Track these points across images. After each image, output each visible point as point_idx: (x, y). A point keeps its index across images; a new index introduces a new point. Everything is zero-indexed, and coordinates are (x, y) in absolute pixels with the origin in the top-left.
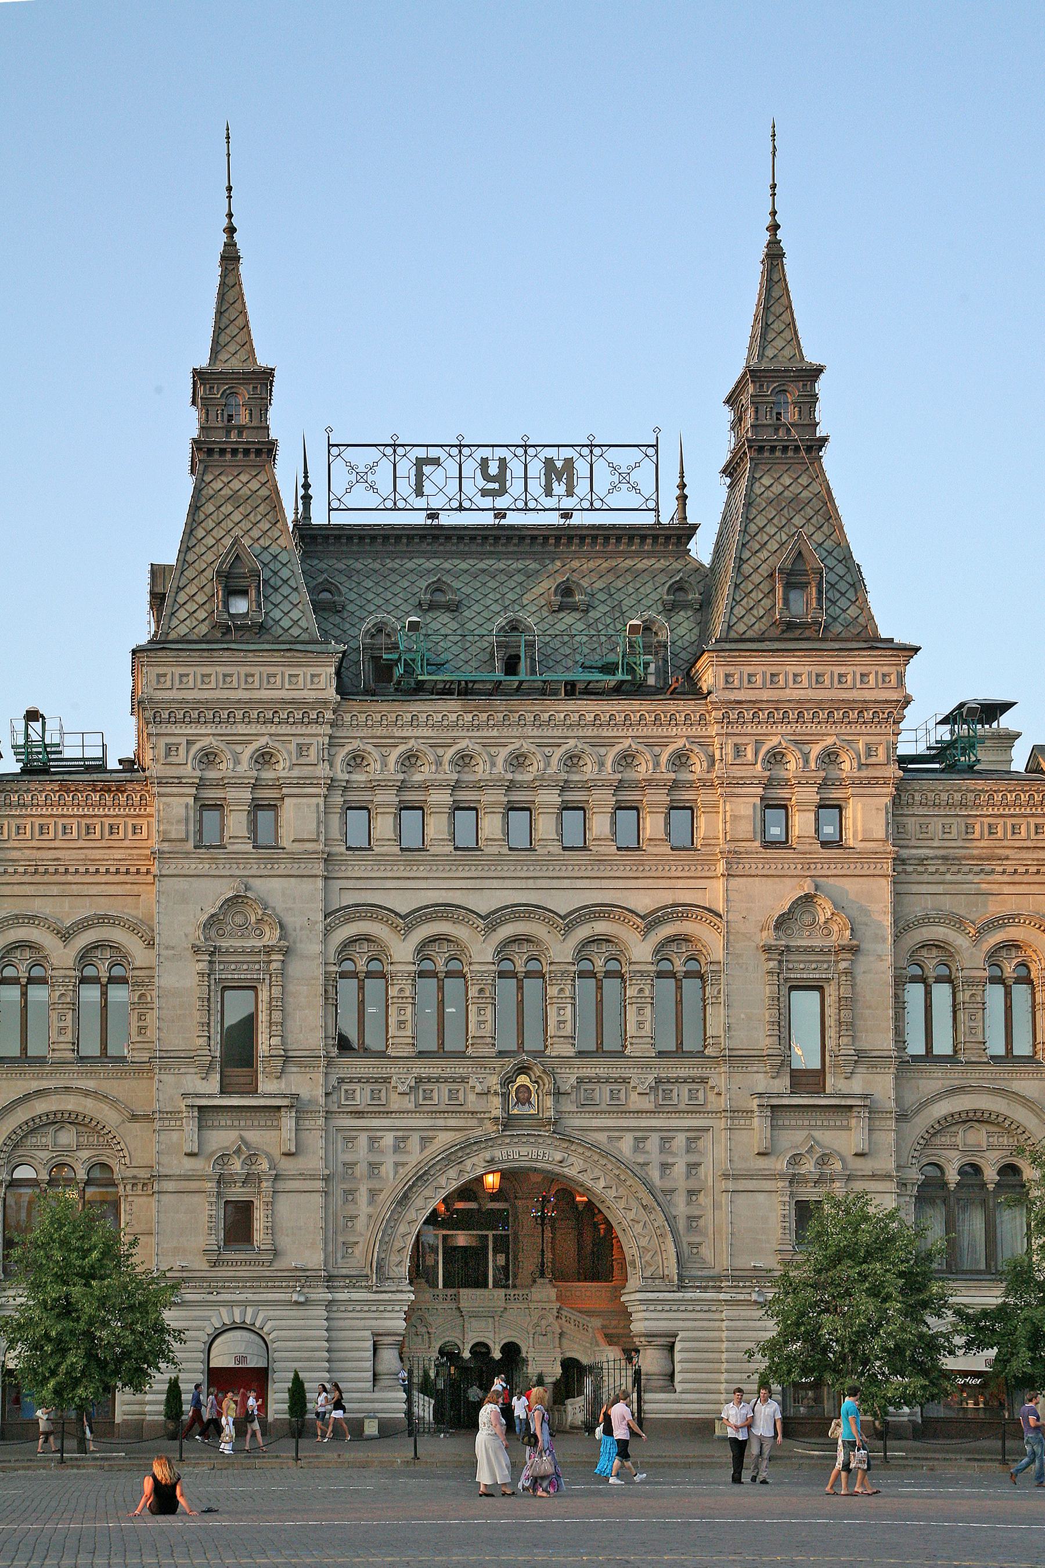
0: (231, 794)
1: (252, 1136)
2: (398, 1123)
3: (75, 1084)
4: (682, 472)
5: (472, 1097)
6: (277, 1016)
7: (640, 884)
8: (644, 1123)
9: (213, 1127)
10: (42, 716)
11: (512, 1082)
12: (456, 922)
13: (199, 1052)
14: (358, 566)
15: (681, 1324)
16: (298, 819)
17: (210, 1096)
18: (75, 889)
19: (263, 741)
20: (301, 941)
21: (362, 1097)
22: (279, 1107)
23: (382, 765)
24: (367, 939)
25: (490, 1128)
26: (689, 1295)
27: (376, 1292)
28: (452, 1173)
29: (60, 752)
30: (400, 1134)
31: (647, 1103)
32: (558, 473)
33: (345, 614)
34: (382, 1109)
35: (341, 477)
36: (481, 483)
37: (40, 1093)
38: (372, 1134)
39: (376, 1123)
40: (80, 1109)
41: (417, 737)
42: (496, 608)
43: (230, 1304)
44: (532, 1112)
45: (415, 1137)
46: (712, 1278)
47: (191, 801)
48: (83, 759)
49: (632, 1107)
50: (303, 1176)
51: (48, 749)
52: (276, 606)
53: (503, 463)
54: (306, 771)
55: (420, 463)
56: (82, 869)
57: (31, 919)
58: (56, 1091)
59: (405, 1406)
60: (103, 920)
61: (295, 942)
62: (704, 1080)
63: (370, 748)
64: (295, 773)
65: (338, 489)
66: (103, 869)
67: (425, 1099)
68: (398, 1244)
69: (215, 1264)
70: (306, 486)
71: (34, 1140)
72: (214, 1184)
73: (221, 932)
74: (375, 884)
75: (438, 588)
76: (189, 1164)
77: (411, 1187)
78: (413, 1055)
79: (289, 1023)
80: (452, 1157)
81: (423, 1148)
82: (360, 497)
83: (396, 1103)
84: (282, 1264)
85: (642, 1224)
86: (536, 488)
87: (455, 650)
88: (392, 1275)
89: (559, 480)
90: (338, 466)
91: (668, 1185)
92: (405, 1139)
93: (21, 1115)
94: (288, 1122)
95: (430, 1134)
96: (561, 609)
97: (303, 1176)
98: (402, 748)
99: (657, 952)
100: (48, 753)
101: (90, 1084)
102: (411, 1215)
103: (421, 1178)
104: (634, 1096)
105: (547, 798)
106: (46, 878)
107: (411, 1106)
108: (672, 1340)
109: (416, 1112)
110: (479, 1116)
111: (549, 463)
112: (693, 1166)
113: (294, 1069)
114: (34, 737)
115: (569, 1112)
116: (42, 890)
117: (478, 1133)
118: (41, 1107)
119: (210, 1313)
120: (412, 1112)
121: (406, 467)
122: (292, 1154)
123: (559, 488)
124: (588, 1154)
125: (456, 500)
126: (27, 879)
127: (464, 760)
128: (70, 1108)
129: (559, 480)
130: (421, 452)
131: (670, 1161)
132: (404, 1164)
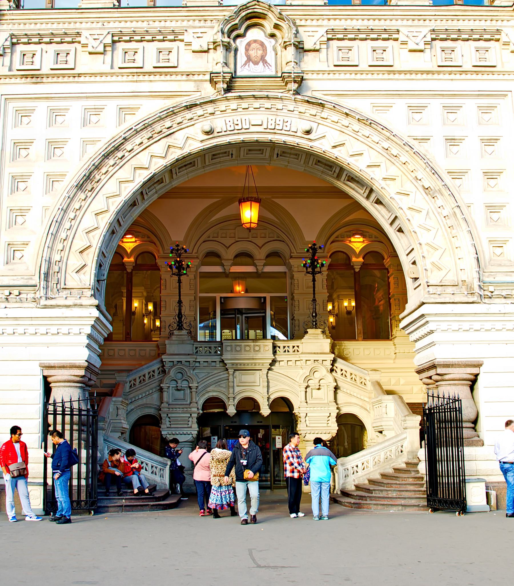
11: (238, 36)
25: (209, 91)
26: (494, 308)
27: (45, 307)
68: (79, 243)
77: (98, 167)
83: (86, 63)
85: (424, 212)
88: (69, 285)
92: (98, 111)
102: (99, 203)
107: (106, 68)
108: (475, 371)
110: (196, 77)
115: (318, 72)
120: (106, 74)
132: (93, 142)
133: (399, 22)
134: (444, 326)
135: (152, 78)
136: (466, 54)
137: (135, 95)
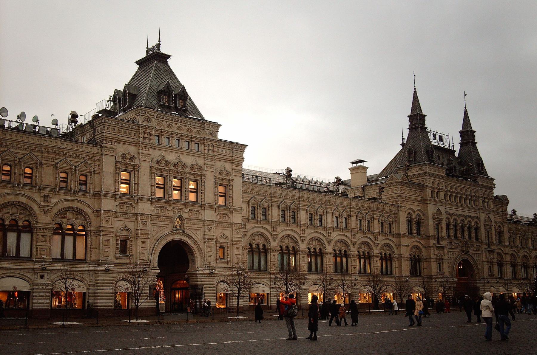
22: (443, 247)
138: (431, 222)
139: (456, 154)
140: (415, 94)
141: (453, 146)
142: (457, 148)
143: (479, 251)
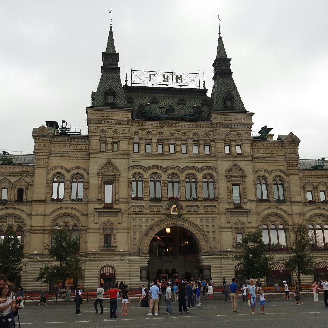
0: (108, 140)
1: (111, 219)
2: (145, 216)
3: (69, 206)
4: (204, 79)
5: (163, 210)
6: (117, 190)
7: (200, 161)
8: (202, 216)
9: (102, 217)
10: (66, 123)
12: (158, 169)
13: (99, 199)
14: (137, 94)
15: (212, 263)
16: (123, 145)
17: (100, 209)
18: (71, 161)
19: (115, 128)
20: (123, 173)
21: (137, 210)
22: (117, 212)
23: (143, 133)
24: (139, 173)
26: (214, 256)
27: (141, 257)
28: (158, 228)
29: (70, 131)
30: (146, 218)
31: (202, 211)
32: (179, 78)
33: (134, 104)
34: (142, 212)
35: (134, 77)
36: (163, 79)
37: (61, 208)
38: (140, 218)
39: (140, 216)
40: (71, 212)
41: (150, 128)
42: (166, 103)
43: (106, 260)
44: (176, 213)
45: (150, 219)
46: (218, 252)
47: (98, 141)
48: (76, 133)
49: (199, 212)
50: (123, 228)
51: (67, 130)
52: (119, 100)
53: (168, 76)
54: (124, 135)
55: (150, 75)
56: (73, 156)
57: (61, 167)
58: (66, 208)
59: (148, 285)
60: (78, 168)
61: (122, 173)
62: (215, 206)
63: (139, 131)
64: (122, 135)
65: (133, 79)
66: (78, 156)
67: (152, 210)
68: (145, 245)
69: (102, 250)
70: (126, 78)
71: (60, 220)
72: (102, 230)
73: (105, 171)
74: (140, 161)
75: (155, 99)
76: (96, 226)
78: (149, 200)
79: (120, 192)
80: (158, 224)
81: (152, 222)
82: (138, 81)
84: (117, 250)
86: (175, 81)
87: (158, 111)
89: (179, 79)
90: (133, 75)
91: (208, 230)
92: (147, 220)
93: (57, 213)
94: (120, 216)
95: (153, 218)
96: (181, 104)
97: (123, 228)
98: (146, 131)
99: (203, 177)
100: (67, 131)
101: (74, 206)
102: (148, 238)
103: (151, 228)
104: (199, 210)
105: (178, 142)
106: (65, 158)
109: (150, 213)
111: (177, 76)
112: (213, 226)
113: (121, 203)
114: (63, 126)
116: (64, 160)
117: (164, 218)
118: (62, 211)
119: (101, 262)
121: (148, 76)
122: (121, 223)
123: (179, 81)
124: (189, 223)
125: (157, 82)
126: (60, 158)
127: (160, 134)
128: (68, 212)
129: (179, 79)
130: (151, 73)
131: (208, 224)
132: (147, 226)
133: (199, 204)
134: (205, 260)
135: (157, 214)
136: (210, 210)
137: (154, 217)
138: (94, 181)
139: (209, 94)
140: (111, 33)
141: (204, 84)
142: (210, 86)
143: (213, 213)
